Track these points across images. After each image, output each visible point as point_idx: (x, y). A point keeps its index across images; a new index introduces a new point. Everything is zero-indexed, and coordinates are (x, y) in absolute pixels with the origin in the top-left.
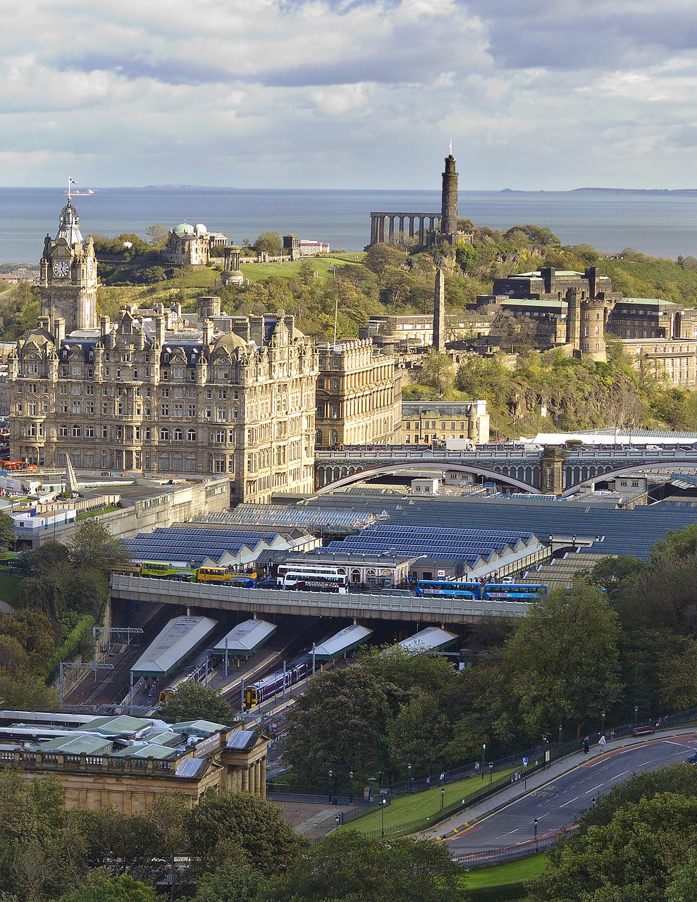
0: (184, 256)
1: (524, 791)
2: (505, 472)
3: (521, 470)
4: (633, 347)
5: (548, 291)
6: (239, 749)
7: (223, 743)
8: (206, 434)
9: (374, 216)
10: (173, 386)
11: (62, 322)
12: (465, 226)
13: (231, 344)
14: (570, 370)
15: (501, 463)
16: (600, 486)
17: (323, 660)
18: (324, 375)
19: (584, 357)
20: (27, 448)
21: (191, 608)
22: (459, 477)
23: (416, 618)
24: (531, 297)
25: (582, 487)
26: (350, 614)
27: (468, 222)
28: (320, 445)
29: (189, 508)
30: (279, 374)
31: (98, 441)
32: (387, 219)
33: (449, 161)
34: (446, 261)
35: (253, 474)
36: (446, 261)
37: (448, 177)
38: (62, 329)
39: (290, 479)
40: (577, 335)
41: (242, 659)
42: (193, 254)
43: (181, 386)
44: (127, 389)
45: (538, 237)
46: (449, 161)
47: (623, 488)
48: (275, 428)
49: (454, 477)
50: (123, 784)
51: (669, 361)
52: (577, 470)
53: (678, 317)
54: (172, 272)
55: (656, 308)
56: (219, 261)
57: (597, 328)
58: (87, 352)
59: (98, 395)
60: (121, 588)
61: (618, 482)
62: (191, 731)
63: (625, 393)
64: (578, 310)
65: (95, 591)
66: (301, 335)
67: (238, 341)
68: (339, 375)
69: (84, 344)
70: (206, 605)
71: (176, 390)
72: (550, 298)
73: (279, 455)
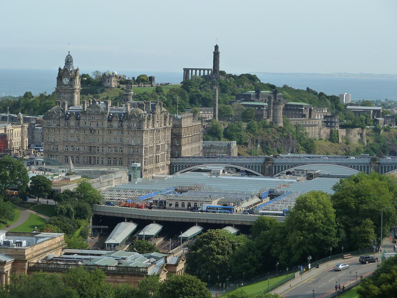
0: (109, 83)
2: (249, 167)
4: (294, 121)
5: (258, 99)
6: (173, 265)
7: (166, 262)
8: (127, 150)
9: (185, 69)
10: (113, 130)
11: (66, 102)
12: (223, 73)
13: (138, 112)
14: (269, 129)
16: (288, 173)
17: (185, 239)
18: (174, 126)
19: (275, 125)
20: (51, 155)
21: (127, 218)
23: (223, 222)
24: (251, 101)
25: (281, 173)
26: (194, 221)
28: (173, 156)
29: (121, 180)
30: (157, 126)
31: (81, 152)
32: (190, 71)
33: (216, 47)
34: (215, 87)
35: (147, 167)
36: (215, 87)
37: (216, 55)
38: (66, 106)
39: (161, 170)
40: (272, 116)
42: (113, 83)
44: (94, 131)
45: (252, 78)
46: (216, 47)
48: (155, 148)
50: (124, 279)
51: (307, 128)
52: (279, 166)
53: (310, 110)
54: (104, 90)
55: (302, 106)
56: (124, 86)
57: (280, 113)
58: (77, 116)
59: (82, 134)
60: (97, 210)
61: (296, 172)
63: (291, 139)
64: (272, 105)
65: (86, 211)
66: (165, 110)
67: (140, 111)
68: (180, 127)
69: (76, 112)
70: (133, 217)
71: (114, 131)
72: (259, 102)
73: (156, 159)
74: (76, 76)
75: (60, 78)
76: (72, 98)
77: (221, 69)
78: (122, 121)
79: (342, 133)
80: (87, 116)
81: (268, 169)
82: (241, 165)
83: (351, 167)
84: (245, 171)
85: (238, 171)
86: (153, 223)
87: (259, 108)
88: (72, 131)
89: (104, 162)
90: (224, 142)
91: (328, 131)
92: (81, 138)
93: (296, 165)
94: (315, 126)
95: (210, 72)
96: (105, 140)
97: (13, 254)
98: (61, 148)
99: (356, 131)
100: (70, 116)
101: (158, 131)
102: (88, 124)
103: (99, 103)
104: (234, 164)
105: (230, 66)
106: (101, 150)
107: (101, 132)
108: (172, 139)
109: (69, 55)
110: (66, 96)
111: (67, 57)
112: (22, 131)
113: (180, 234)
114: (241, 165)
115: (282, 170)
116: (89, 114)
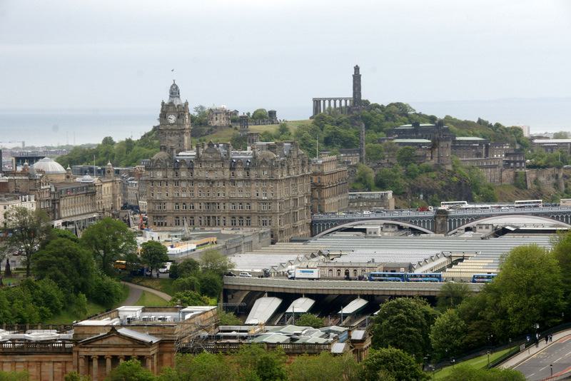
0: (218, 121)
1: (529, 355)
3: (424, 221)
5: (417, 134)
6: (358, 340)
10: (238, 181)
12: (367, 102)
15: (413, 218)
16: (468, 229)
17: (345, 316)
22: (390, 227)
23: (393, 293)
24: (407, 138)
26: (356, 293)
27: (367, 101)
33: (357, 69)
41: (298, 318)
43: (241, 180)
46: (357, 69)
47: (481, 230)
48: (292, 202)
49: (387, 227)
52: (455, 220)
53: (487, 147)
60: (229, 283)
61: (478, 228)
62: (330, 331)
70: (276, 291)
73: (294, 217)
74: (185, 112)
75: (163, 116)
76: (182, 140)
77: (362, 98)
78: (249, 169)
79: (531, 175)
80: (203, 163)
81: (443, 224)
82: (404, 220)
83: (553, 218)
84: (410, 228)
85: (400, 228)
86: (302, 297)
87: (421, 147)
88: (183, 185)
89: (227, 223)
90: (377, 194)
91: (512, 174)
92: (196, 193)
93: (478, 217)
94: (495, 167)
95: (348, 101)
96: (227, 194)
97: (159, 332)
98: (170, 207)
99: (549, 171)
100: (180, 164)
101: (296, 179)
102: (203, 175)
103: (218, 146)
104: (396, 219)
105: (376, 94)
106: (222, 208)
107: (221, 184)
108: (312, 190)
109: (174, 84)
110: (172, 138)
111: (172, 87)
112: (113, 187)
113: (340, 310)
114: (404, 220)
115: (459, 226)
116: (205, 161)
